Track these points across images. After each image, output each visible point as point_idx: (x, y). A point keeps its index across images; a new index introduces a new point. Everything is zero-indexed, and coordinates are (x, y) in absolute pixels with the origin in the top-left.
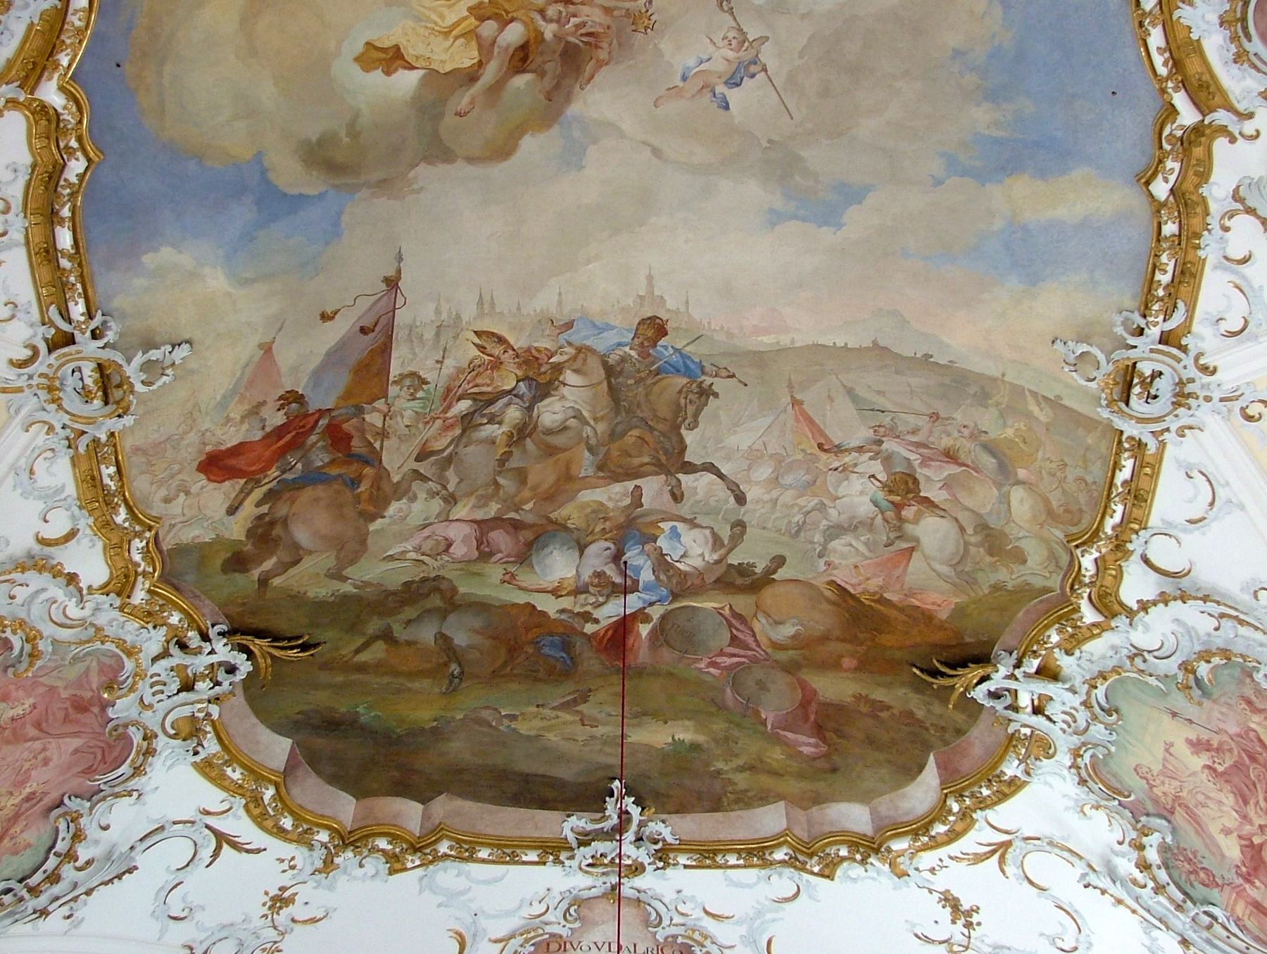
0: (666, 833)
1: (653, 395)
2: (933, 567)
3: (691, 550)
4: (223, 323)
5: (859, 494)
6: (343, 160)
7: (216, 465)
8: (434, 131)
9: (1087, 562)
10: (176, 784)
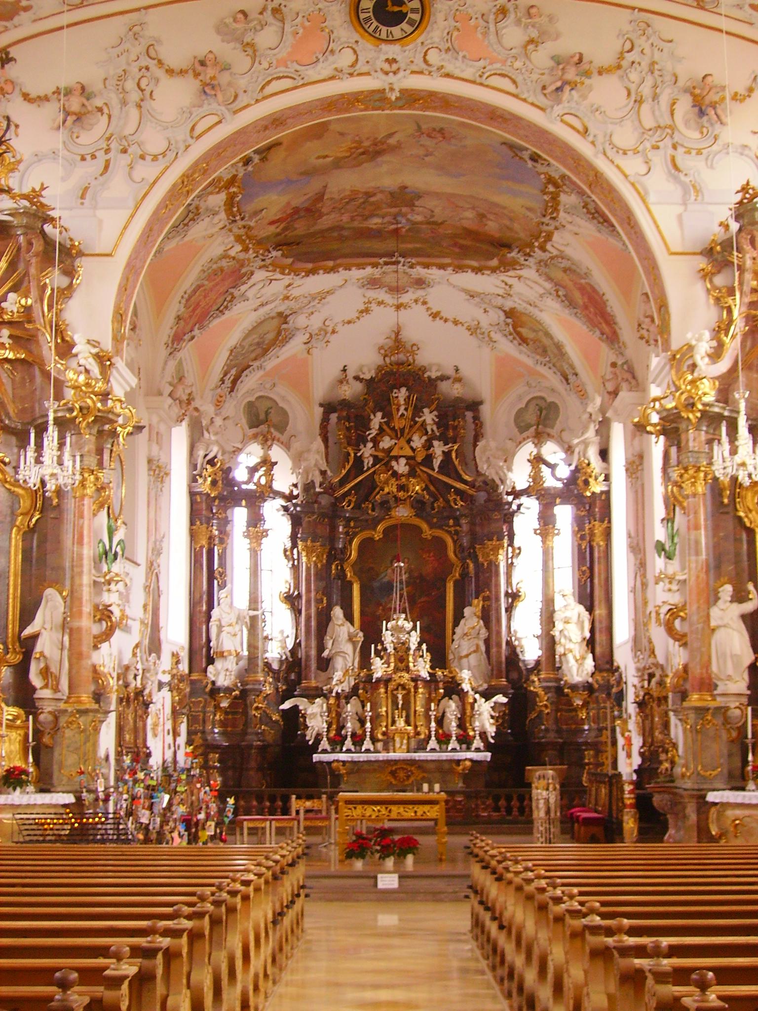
0: (413, 261)
1: (404, 198)
2: (492, 227)
3: (419, 218)
4: (273, 203)
5: (469, 214)
6: (310, 173)
7: (272, 223)
8: (338, 164)
9: (536, 244)
10: (260, 275)
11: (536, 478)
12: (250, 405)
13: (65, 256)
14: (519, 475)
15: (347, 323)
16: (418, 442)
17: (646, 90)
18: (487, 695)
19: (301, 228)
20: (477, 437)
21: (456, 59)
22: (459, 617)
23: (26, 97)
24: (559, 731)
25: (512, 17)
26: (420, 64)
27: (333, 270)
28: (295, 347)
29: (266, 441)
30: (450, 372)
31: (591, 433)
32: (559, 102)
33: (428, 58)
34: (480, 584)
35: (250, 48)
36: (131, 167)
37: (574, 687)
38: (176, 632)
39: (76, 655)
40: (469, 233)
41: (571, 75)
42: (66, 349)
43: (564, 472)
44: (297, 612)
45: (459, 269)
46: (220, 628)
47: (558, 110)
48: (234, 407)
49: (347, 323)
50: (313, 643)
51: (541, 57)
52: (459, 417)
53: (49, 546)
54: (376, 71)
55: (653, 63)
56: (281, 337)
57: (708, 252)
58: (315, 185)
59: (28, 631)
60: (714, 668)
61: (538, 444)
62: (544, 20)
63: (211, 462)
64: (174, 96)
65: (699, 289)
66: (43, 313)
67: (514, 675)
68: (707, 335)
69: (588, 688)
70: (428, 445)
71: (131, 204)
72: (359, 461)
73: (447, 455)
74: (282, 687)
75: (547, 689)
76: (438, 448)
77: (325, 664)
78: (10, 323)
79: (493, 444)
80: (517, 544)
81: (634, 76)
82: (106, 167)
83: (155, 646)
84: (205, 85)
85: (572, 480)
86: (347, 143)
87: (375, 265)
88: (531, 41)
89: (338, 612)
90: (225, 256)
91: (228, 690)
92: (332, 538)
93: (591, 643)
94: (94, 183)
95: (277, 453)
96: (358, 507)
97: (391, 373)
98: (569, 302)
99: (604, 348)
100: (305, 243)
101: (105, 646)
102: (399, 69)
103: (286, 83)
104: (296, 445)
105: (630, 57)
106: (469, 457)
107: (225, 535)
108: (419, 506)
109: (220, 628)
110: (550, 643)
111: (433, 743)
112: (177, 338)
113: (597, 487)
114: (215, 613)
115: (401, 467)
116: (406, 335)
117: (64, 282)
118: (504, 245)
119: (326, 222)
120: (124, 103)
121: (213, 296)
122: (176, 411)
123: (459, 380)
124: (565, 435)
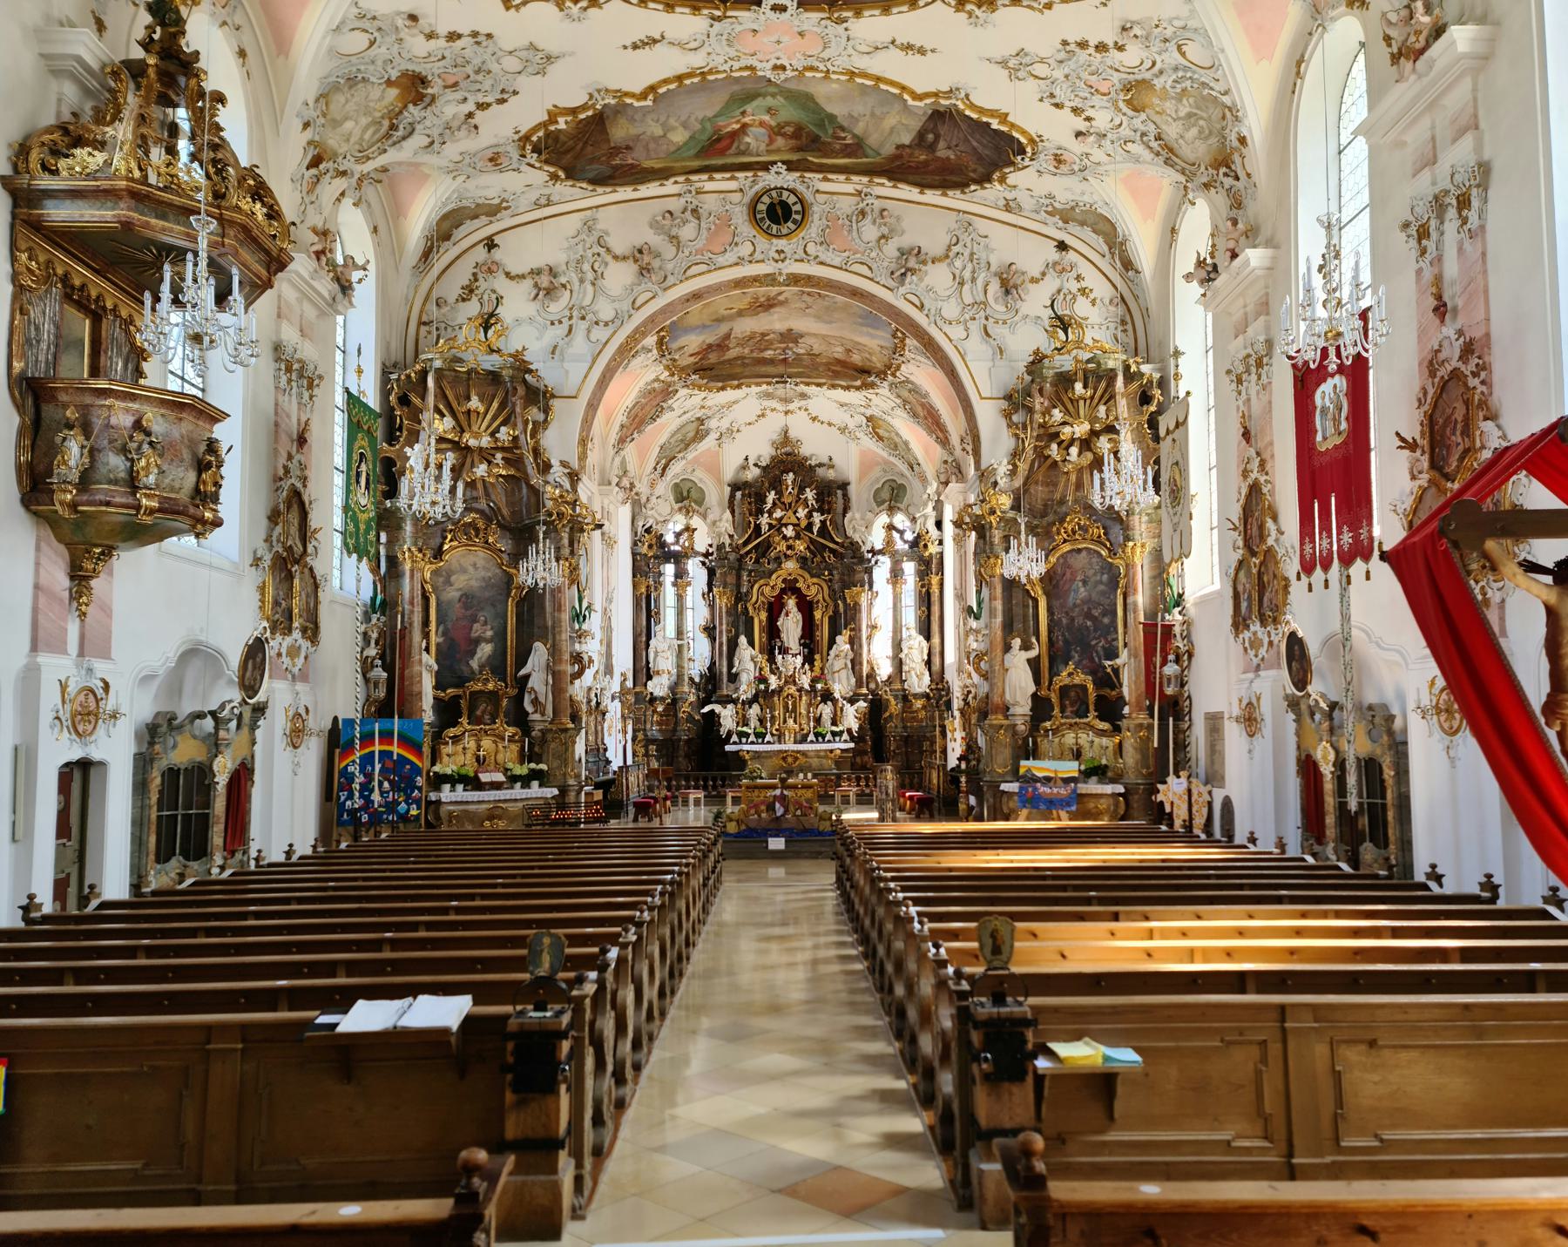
1: (790, 337)
2: (856, 358)
4: (693, 342)
5: (840, 349)
6: (719, 320)
8: (740, 313)
10: (683, 392)
11: (889, 542)
12: (676, 485)
13: (539, 397)
14: (876, 538)
15: (748, 425)
16: (802, 513)
17: (967, 275)
18: (852, 701)
19: (713, 358)
20: (846, 509)
22: (832, 642)
23: (507, 274)
24: (905, 727)
25: (869, 218)
26: (801, 254)
27: (739, 387)
28: (709, 442)
29: (688, 512)
30: (826, 460)
31: (929, 509)
32: (902, 283)
34: (846, 618)
35: (674, 239)
36: (589, 331)
37: (916, 696)
38: (623, 660)
39: (558, 689)
40: (839, 362)
41: (909, 263)
42: (546, 467)
43: (909, 536)
44: (713, 639)
45: (834, 386)
46: (656, 653)
47: (902, 290)
48: (664, 488)
49: (748, 425)
50: (725, 663)
51: (891, 249)
52: (831, 494)
53: (536, 611)
55: (972, 254)
56: (700, 435)
57: (1008, 397)
58: (723, 329)
59: (522, 672)
60: (1008, 697)
61: (891, 515)
62: (892, 220)
63: (648, 531)
64: (619, 276)
65: (1004, 423)
66: (527, 442)
67: (872, 686)
68: (1005, 462)
69: (926, 696)
70: (809, 515)
71: (590, 359)
72: (758, 527)
73: (823, 523)
74: (702, 695)
75: (896, 697)
76: (817, 518)
77: (734, 678)
78: (503, 449)
79: (857, 516)
80: (875, 589)
81: (958, 263)
82: (570, 331)
83: (609, 670)
84: (642, 268)
85: (915, 544)
86: (748, 299)
87: (769, 384)
88: (883, 237)
89: (743, 640)
90: (657, 380)
91: (663, 699)
92: (738, 585)
93: (929, 663)
94: (561, 343)
95: (696, 522)
96: (757, 561)
97: (782, 462)
98: (915, 415)
99: (938, 448)
100: (716, 369)
101: (577, 682)
103: (703, 268)
104: (711, 517)
105: (955, 249)
106: (839, 522)
107: (659, 584)
108: (803, 561)
109: (656, 653)
110: (899, 664)
111: (811, 737)
112: (622, 441)
113: (933, 549)
114: (652, 642)
115: (789, 532)
116: (792, 434)
117: (541, 417)
118: (868, 372)
119: (732, 354)
120: (582, 281)
121: (648, 408)
122: (621, 495)
123: (832, 467)
124: (911, 509)
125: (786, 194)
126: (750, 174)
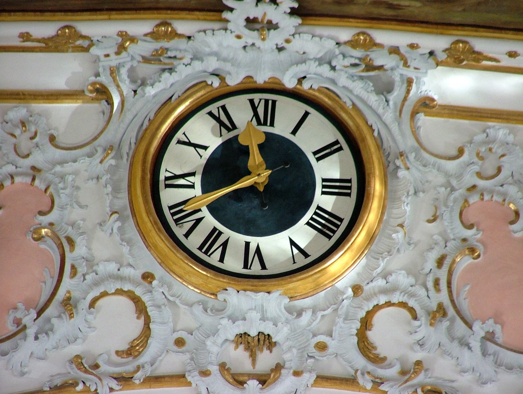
21: (465, 344)
33: (372, 335)
54: (205, 373)
102: (278, 368)
125: (288, 112)
126: (140, 27)
